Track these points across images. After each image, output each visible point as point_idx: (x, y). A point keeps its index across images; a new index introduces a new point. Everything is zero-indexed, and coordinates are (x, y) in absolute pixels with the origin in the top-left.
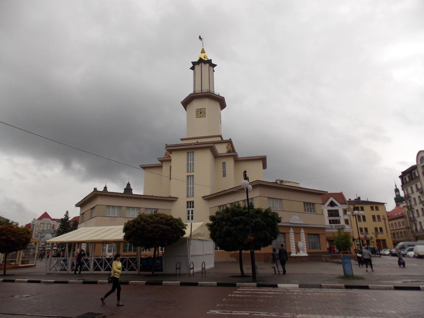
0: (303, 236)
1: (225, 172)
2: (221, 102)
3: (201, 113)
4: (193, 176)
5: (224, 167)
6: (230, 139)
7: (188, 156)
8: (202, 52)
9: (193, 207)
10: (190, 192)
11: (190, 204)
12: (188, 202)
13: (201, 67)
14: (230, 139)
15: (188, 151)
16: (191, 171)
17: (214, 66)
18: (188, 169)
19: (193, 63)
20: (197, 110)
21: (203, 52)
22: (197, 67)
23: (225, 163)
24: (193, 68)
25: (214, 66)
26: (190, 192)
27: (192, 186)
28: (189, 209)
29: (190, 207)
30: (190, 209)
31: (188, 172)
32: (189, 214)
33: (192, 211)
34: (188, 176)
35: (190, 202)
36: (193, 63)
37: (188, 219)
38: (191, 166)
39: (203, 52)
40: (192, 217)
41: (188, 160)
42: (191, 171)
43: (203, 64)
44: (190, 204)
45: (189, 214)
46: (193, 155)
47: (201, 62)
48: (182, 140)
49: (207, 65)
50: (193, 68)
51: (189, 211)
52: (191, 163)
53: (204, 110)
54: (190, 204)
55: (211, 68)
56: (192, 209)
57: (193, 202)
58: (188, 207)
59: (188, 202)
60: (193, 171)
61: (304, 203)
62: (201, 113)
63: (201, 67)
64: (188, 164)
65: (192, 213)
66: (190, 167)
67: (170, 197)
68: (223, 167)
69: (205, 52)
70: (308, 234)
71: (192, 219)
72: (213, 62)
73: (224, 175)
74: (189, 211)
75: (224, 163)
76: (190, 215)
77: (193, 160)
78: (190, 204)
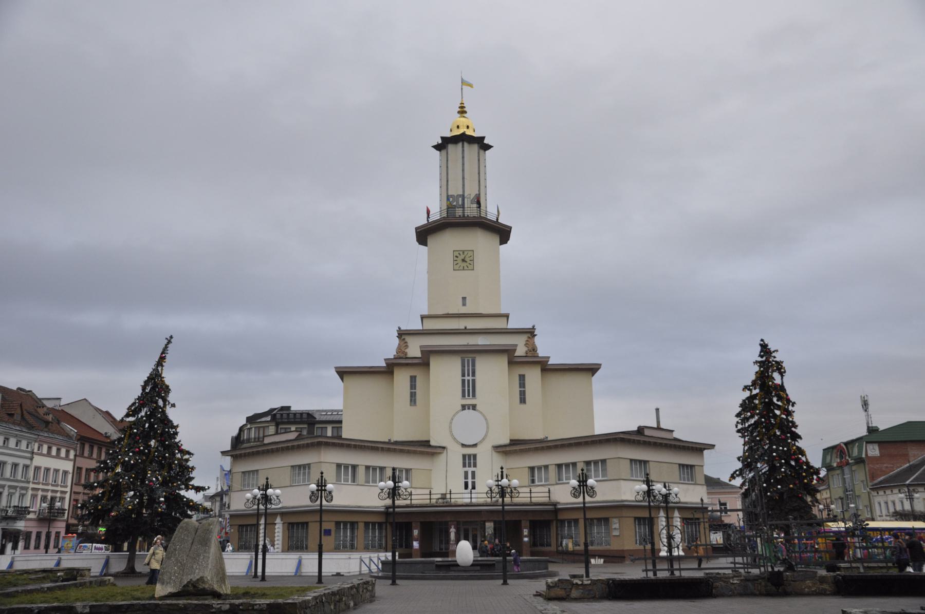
0: (677, 522)
1: (524, 394)
2: (503, 234)
3: (464, 260)
5: (522, 384)
6: (533, 328)
7: (463, 366)
8: (459, 112)
9: (475, 466)
11: (470, 459)
12: (464, 456)
13: (463, 151)
14: (533, 328)
15: (464, 356)
17: (488, 147)
18: (463, 391)
19: (442, 138)
21: (462, 111)
22: (451, 147)
23: (524, 376)
24: (438, 147)
25: (488, 147)
28: (467, 469)
29: (470, 466)
30: (470, 470)
31: (464, 396)
32: (466, 477)
35: (469, 456)
36: (442, 138)
37: (466, 487)
38: (469, 386)
39: (462, 111)
40: (474, 483)
41: (463, 375)
43: (466, 144)
44: (470, 459)
45: (466, 477)
46: (474, 365)
47: (463, 141)
48: (423, 318)
49: (475, 147)
50: (438, 147)
51: (466, 473)
53: (470, 253)
55: (482, 152)
56: (473, 469)
57: (475, 456)
58: (464, 466)
60: (474, 395)
61: (680, 465)
62: (463, 260)
63: (463, 151)
64: (463, 381)
65: (473, 477)
66: (469, 389)
67: (430, 446)
69: (466, 112)
70: (686, 519)
71: (474, 488)
72: (486, 141)
73: (523, 400)
74: (466, 473)
75: (522, 378)
76: (470, 481)
77: (474, 375)
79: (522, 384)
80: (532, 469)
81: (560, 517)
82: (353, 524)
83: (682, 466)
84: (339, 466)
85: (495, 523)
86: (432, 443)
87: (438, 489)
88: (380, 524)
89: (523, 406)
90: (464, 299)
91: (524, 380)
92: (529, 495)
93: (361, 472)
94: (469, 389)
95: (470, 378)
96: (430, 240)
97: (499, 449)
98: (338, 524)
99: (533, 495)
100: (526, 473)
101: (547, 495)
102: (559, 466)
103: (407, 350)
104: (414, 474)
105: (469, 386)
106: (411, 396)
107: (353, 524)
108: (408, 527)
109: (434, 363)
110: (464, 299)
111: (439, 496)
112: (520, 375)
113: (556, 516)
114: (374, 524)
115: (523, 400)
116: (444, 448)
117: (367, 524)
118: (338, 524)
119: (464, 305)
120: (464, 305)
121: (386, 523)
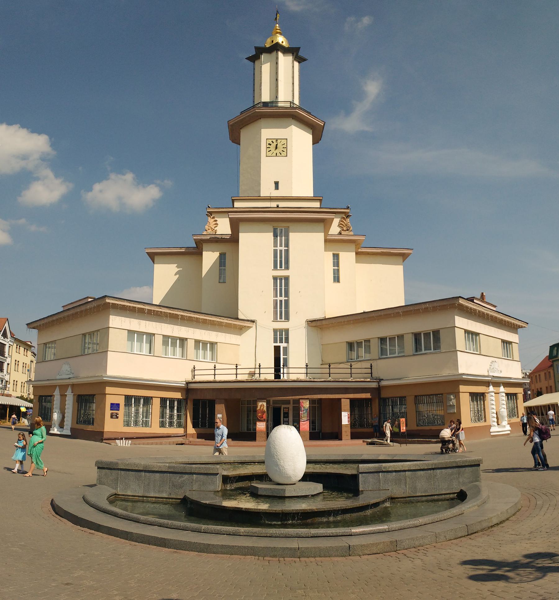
4: (287, 279)
5: (336, 263)
7: (275, 236)
9: (287, 341)
10: (283, 310)
11: (281, 335)
12: (275, 331)
13: (277, 58)
15: (276, 224)
16: (281, 267)
20: (270, 141)
26: (283, 310)
27: (283, 298)
29: (281, 341)
33: (285, 349)
34: (275, 278)
35: (281, 331)
41: (275, 245)
42: (281, 267)
44: (281, 335)
47: (277, 50)
52: (281, 251)
53: (284, 142)
54: (282, 336)
57: (287, 331)
58: (275, 341)
59: (275, 331)
60: (287, 268)
62: (276, 148)
64: (275, 252)
66: (282, 260)
67: (237, 319)
68: (334, 262)
73: (337, 279)
75: (336, 257)
77: (287, 245)
78: (282, 336)
79: (336, 263)
80: (351, 345)
81: (384, 395)
82: (148, 400)
83: (504, 341)
84: (131, 333)
85: (312, 402)
86: (241, 316)
87: (247, 364)
88: (179, 401)
89: (337, 284)
90: (277, 184)
91: (338, 259)
92: (349, 371)
93: (158, 341)
94: (282, 260)
95: (283, 248)
96: (245, 134)
97: (314, 324)
98: (128, 398)
99: (354, 371)
100: (345, 347)
101: (369, 371)
102: (383, 340)
103: (215, 229)
104: (220, 348)
105: (281, 257)
106: (220, 274)
107: (148, 400)
108: (211, 404)
109: (244, 237)
110: (277, 184)
111: (247, 371)
112: (334, 255)
113: (379, 394)
114: (172, 401)
115: (337, 279)
116: (253, 321)
117: (163, 401)
118: (128, 398)
119: (277, 188)
120: (277, 188)
121: (186, 400)
